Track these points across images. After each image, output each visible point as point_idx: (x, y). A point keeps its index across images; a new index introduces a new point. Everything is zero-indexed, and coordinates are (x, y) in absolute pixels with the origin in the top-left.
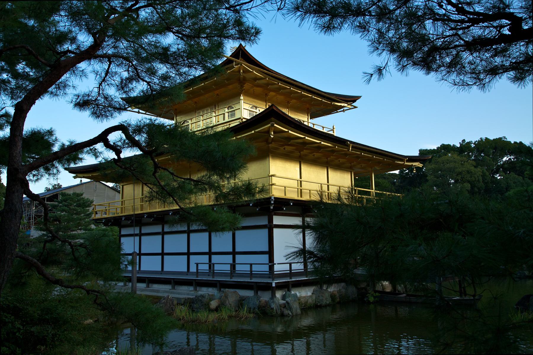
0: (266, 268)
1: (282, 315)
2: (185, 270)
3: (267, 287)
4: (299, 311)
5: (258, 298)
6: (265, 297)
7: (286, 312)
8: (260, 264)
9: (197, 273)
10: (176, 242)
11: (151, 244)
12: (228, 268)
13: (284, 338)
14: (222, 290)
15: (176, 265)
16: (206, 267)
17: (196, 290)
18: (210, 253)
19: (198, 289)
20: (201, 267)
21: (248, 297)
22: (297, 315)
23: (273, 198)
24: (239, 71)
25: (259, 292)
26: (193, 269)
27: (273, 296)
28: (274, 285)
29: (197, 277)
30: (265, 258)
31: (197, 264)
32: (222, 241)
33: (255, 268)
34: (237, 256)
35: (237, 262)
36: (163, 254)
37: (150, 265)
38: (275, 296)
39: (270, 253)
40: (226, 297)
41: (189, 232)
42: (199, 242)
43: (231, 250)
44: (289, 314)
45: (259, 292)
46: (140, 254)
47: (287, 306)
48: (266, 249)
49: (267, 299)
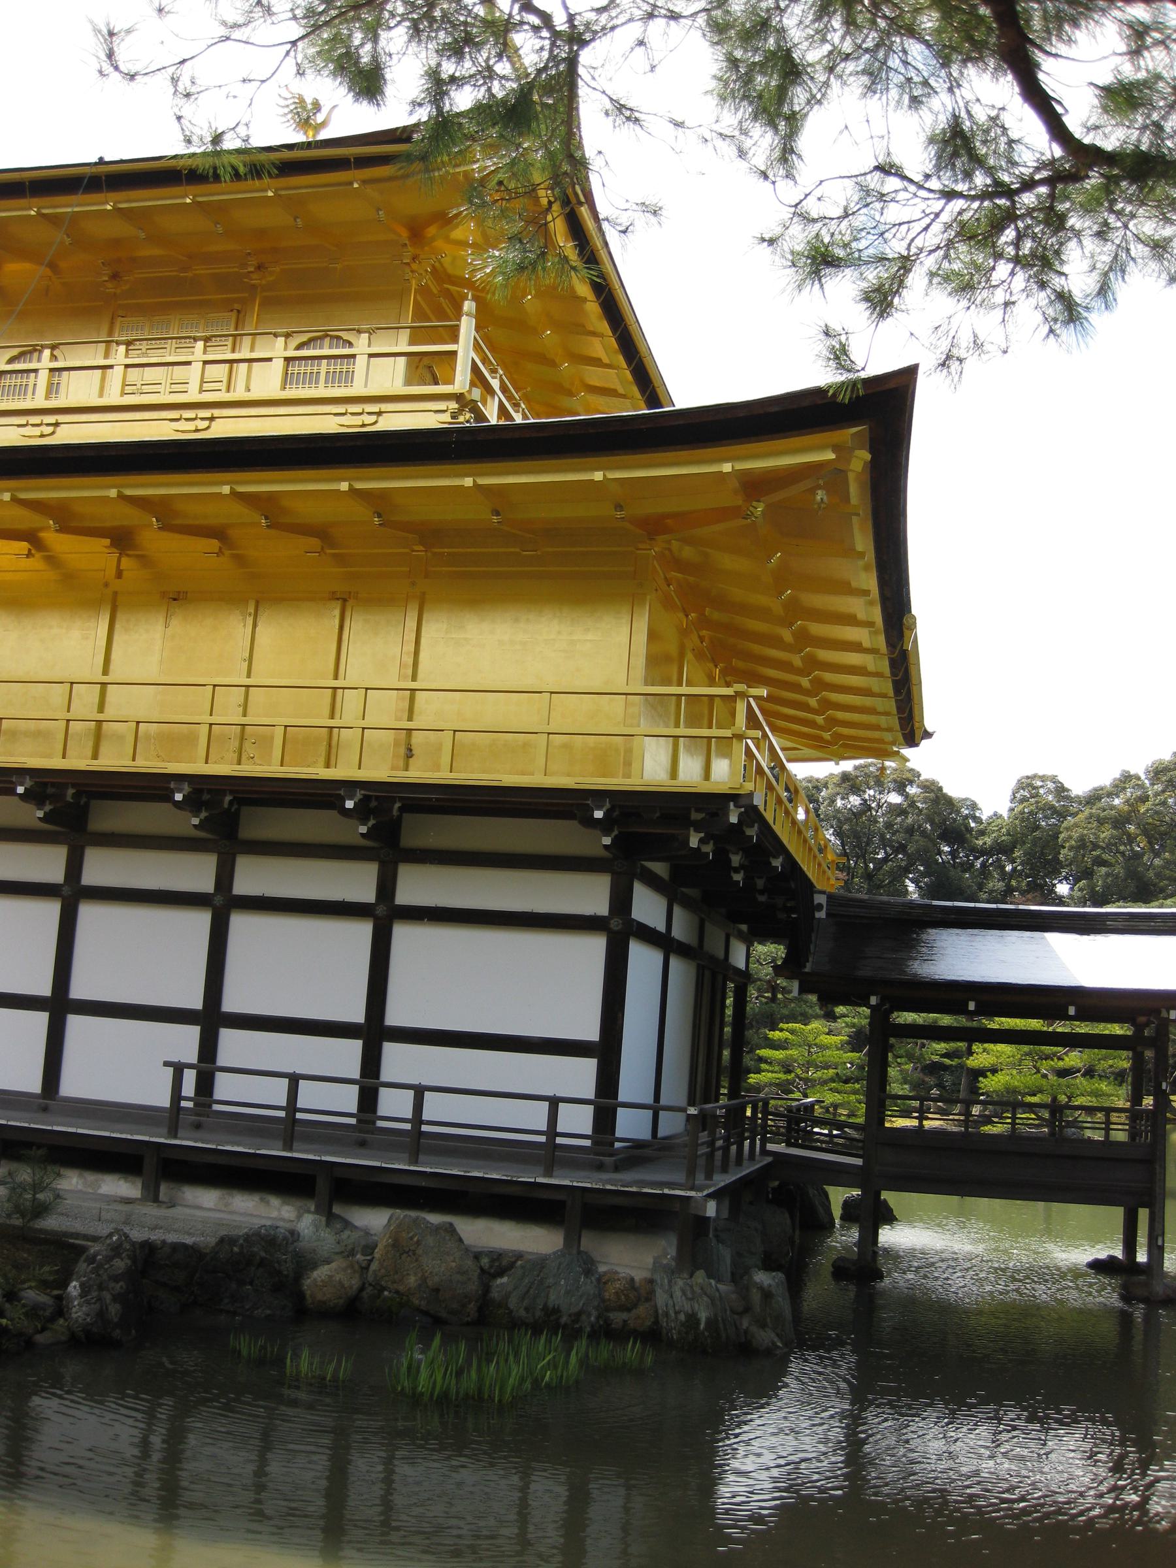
1: (746, 1350)
2: (33, 1084)
6: (629, 1259)
14: (337, 1209)
17: (156, 1199)
19: (162, 1196)
25: (589, 1242)
29: (174, 1133)
30: (579, 1076)
32: (298, 965)
34: (392, 1052)
35: (386, 1075)
39: (606, 1050)
43: (356, 1014)
44: (773, 1343)
48: (590, 1032)
49: (639, 1275)
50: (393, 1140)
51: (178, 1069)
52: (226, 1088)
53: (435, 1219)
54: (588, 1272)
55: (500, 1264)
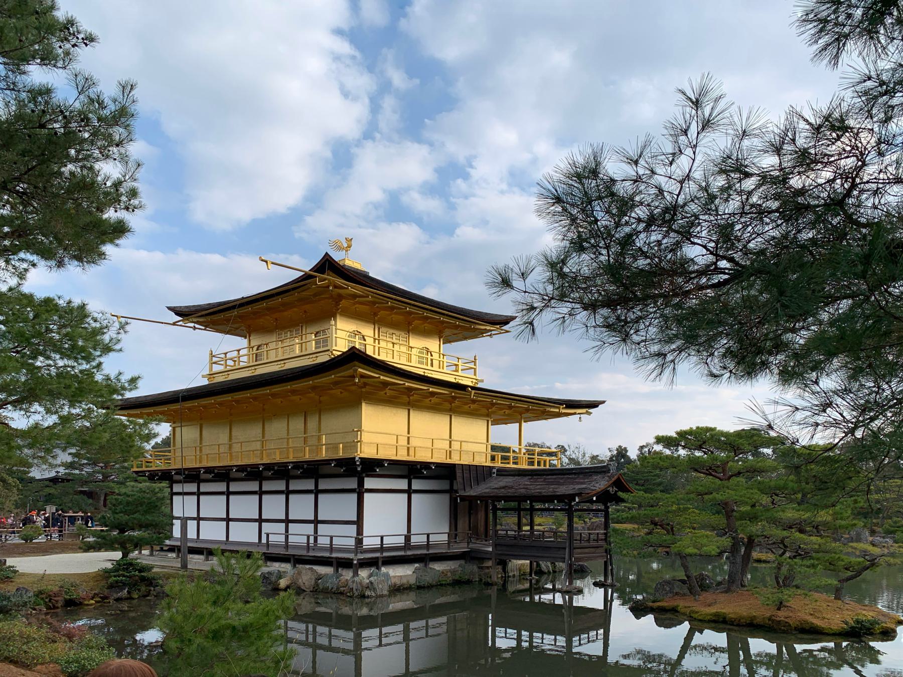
0: (351, 542)
1: (363, 596)
3: (346, 564)
4: (385, 592)
5: (339, 576)
6: (347, 574)
7: (368, 593)
8: (344, 537)
9: (268, 545)
10: (243, 506)
11: (213, 506)
12: (304, 540)
13: (369, 622)
15: (244, 534)
16: (282, 539)
18: (287, 521)
20: (271, 538)
21: (326, 575)
22: (382, 596)
23: (357, 459)
24: (328, 287)
26: (264, 541)
27: (356, 574)
28: (355, 562)
31: (268, 535)
32: (302, 507)
33: (336, 541)
36: (228, 520)
37: (212, 532)
38: (358, 575)
40: (299, 573)
41: (261, 493)
42: (274, 506)
45: (340, 570)
46: (199, 519)
47: (370, 586)
50: (323, 549)
51: (308, 537)
52: (291, 539)
53: (308, 566)
54: (337, 578)
55: (320, 577)
